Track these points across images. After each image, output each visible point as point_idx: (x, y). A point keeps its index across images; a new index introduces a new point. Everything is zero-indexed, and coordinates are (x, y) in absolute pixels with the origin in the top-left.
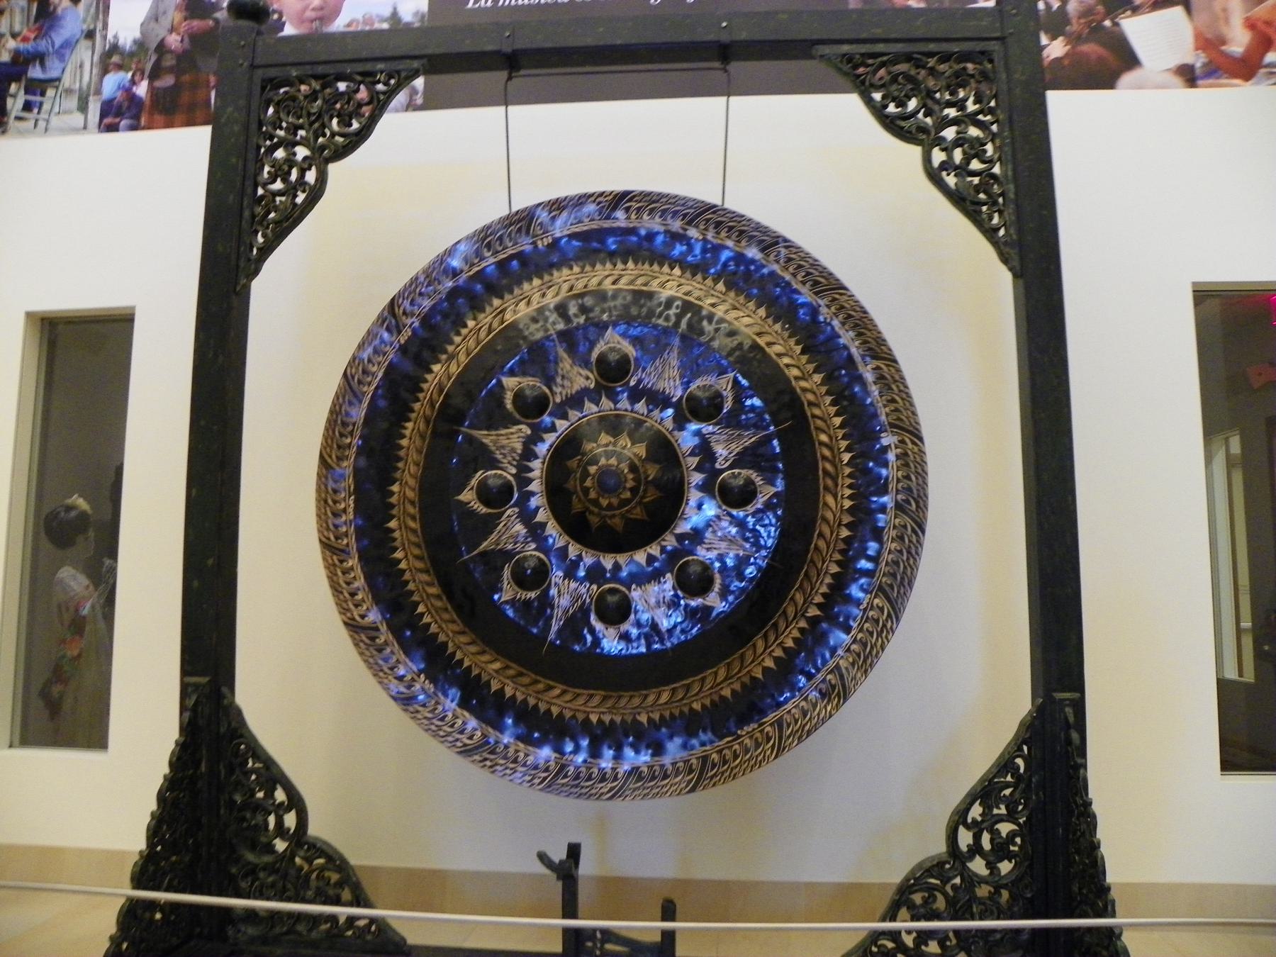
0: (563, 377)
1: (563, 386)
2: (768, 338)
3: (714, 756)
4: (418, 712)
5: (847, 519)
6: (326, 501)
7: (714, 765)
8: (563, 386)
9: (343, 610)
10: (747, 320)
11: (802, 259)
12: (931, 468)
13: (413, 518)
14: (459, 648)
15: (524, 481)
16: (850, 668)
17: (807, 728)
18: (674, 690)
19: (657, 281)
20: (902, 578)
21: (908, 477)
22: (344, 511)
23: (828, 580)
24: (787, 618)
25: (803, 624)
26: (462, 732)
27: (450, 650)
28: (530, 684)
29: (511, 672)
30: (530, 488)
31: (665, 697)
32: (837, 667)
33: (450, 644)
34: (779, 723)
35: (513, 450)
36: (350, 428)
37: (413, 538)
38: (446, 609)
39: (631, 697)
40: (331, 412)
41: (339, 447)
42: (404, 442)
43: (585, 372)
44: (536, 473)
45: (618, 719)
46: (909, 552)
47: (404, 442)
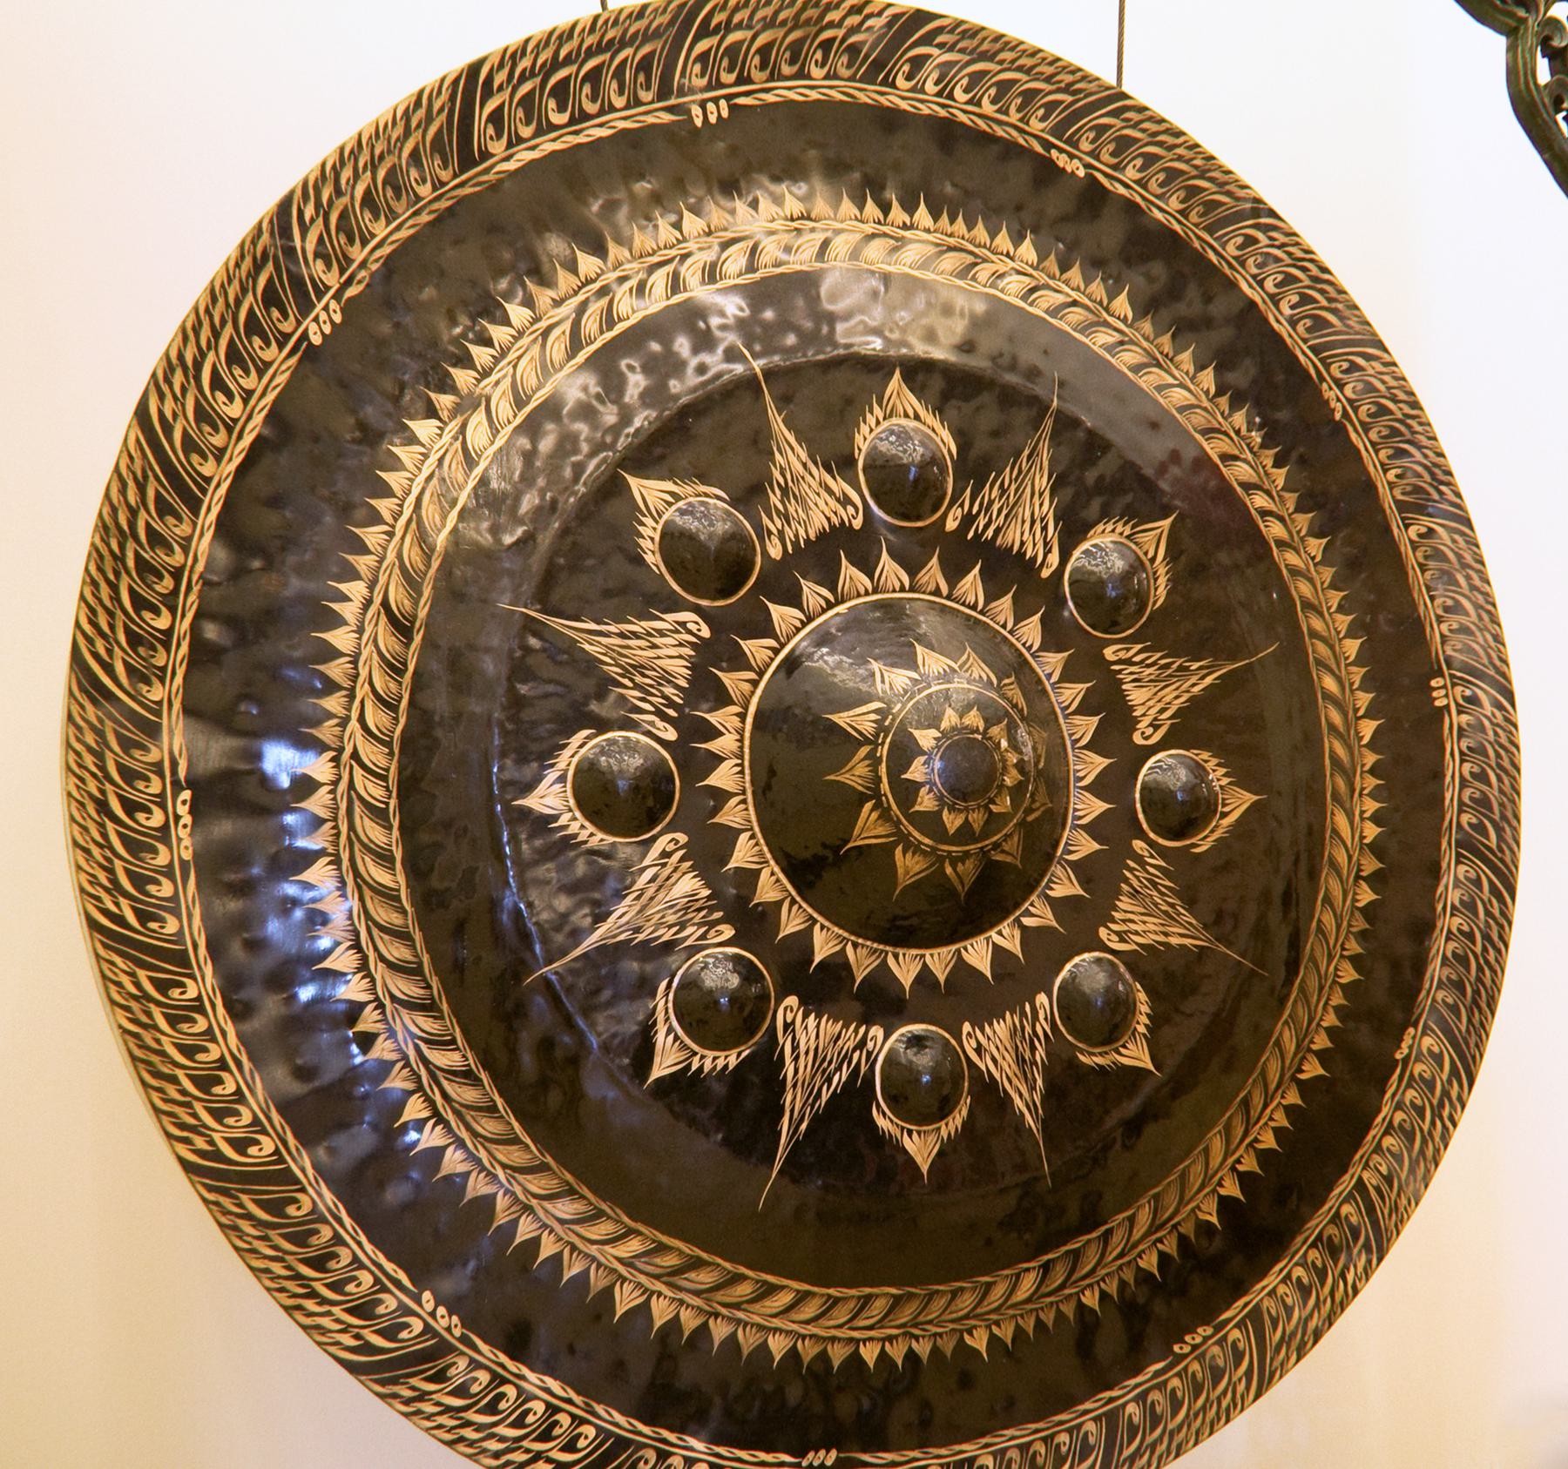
0: (785, 491)
1: (786, 518)
2: (1224, 445)
3: (1132, 1408)
4: (423, 1396)
5: (1371, 865)
6: (103, 806)
7: (1133, 1430)
8: (786, 518)
9: (179, 1130)
10: (1179, 396)
11: (1296, 262)
12: (1526, 759)
13: (384, 858)
14: (527, 1209)
15: (697, 763)
16: (1385, 1188)
17: (1312, 1325)
18: (1046, 1268)
19: (993, 267)
20: (1476, 992)
21: (1482, 777)
22: (164, 833)
23: (1338, 999)
24: (1266, 1086)
25: (1293, 1098)
26: (545, 1436)
27: (501, 1219)
28: (717, 1288)
29: (670, 1261)
30: (714, 780)
31: (1028, 1284)
32: (1360, 1185)
33: (501, 1202)
34: (1256, 1315)
35: (667, 678)
36: (168, 583)
37: (384, 915)
38: (492, 1109)
39: (955, 1294)
40: (103, 528)
41: (134, 640)
42: (341, 639)
43: (839, 485)
44: (724, 744)
45: (923, 1349)
46: (1487, 937)
47: (341, 639)
